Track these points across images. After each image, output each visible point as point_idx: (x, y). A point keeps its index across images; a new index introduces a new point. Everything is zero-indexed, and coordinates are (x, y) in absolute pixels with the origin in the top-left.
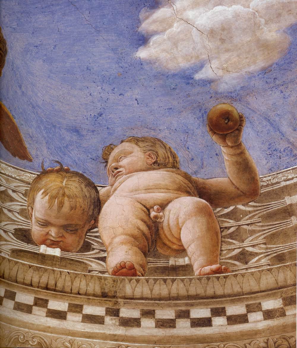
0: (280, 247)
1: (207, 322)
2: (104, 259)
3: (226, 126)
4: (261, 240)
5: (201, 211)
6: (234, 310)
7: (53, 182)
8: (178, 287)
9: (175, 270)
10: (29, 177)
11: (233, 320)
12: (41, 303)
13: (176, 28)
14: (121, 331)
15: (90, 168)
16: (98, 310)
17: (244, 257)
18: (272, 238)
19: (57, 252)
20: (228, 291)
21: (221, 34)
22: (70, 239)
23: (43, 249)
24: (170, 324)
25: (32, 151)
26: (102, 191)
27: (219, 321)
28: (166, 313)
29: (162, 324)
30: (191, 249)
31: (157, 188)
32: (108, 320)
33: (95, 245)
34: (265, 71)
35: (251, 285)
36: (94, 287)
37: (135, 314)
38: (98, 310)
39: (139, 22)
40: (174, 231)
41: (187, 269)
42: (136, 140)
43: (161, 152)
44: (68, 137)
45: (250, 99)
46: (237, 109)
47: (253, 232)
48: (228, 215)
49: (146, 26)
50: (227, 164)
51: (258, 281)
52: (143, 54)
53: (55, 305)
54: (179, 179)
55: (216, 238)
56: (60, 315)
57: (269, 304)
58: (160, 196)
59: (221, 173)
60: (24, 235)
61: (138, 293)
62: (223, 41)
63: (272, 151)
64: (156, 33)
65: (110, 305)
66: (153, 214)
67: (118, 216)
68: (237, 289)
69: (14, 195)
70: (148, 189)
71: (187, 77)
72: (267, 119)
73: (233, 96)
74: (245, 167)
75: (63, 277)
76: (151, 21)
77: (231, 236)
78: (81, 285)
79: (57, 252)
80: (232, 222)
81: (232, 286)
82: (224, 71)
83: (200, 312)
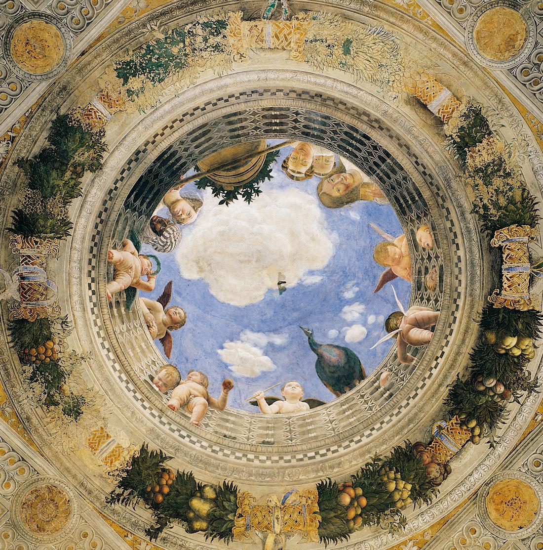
0: (218, 429)
1: (183, 437)
2: (168, 400)
3: (227, 386)
4: (214, 424)
5: (204, 405)
6: (194, 439)
7: (171, 369)
8: (183, 422)
9: (186, 416)
10: (165, 363)
11: (191, 441)
12: (142, 400)
13: (233, 351)
14: (158, 424)
15: (183, 372)
16: (156, 414)
17: (207, 425)
18: (218, 425)
19: (157, 389)
20: (196, 432)
21: (243, 360)
22: (164, 388)
23: (154, 386)
24: (173, 431)
25: (171, 357)
26: (182, 381)
27: (187, 439)
28: (174, 427)
29: (171, 429)
30: (194, 413)
31: (197, 390)
32: (157, 418)
33: (169, 395)
34: (248, 378)
35: (203, 434)
36: (160, 406)
37: (166, 422)
38: (156, 414)
39: (225, 342)
40: (193, 405)
41: (189, 418)
42: (201, 373)
43: (205, 381)
44: (184, 360)
45: (239, 383)
46: (234, 383)
47: (214, 420)
48: (210, 411)
49: (225, 345)
50: (220, 397)
51: (206, 435)
52: (219, 351)
53: (146, 404)
54: (205, 392)
55: (203, 415)
56: (145, 408)
57: (204, 444)
58: (196, 393)
59: (217, 398)
60: (152, 378)
61: (170, 416)
62: (243, 362)
63: (235, 401)
64: (227, 348)
65: (160, 414)
66: (191, 397)
67: (180, 392)
68: (198, 433)
69: (157, 365)
70: (194, 389)
71: (226, 366)
72: (240, 391)
73: (235, 379)
74: (224, 401)
75: (153, 398)
76: (227, 344)
77: (207, 417)
78: (157, 403)
79: (157, 389)
80: (210, 413)
81: (197, 431)
82: (237, 371)
83: (184, 433)
